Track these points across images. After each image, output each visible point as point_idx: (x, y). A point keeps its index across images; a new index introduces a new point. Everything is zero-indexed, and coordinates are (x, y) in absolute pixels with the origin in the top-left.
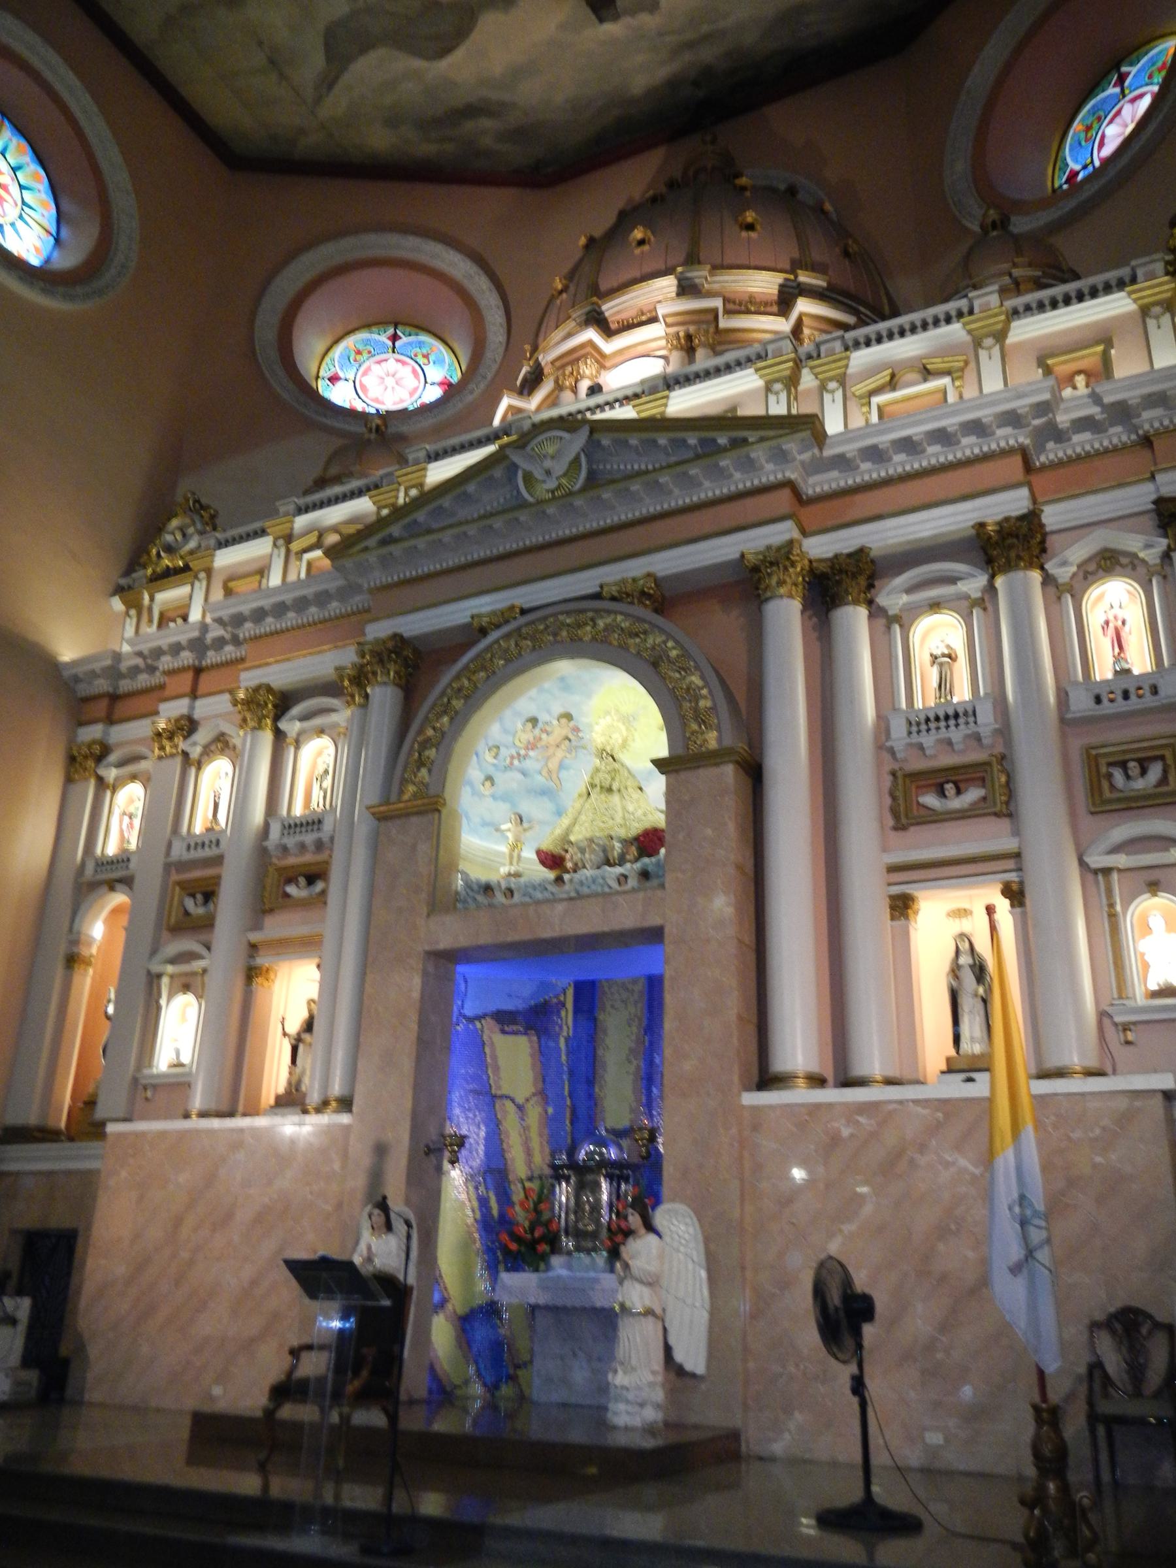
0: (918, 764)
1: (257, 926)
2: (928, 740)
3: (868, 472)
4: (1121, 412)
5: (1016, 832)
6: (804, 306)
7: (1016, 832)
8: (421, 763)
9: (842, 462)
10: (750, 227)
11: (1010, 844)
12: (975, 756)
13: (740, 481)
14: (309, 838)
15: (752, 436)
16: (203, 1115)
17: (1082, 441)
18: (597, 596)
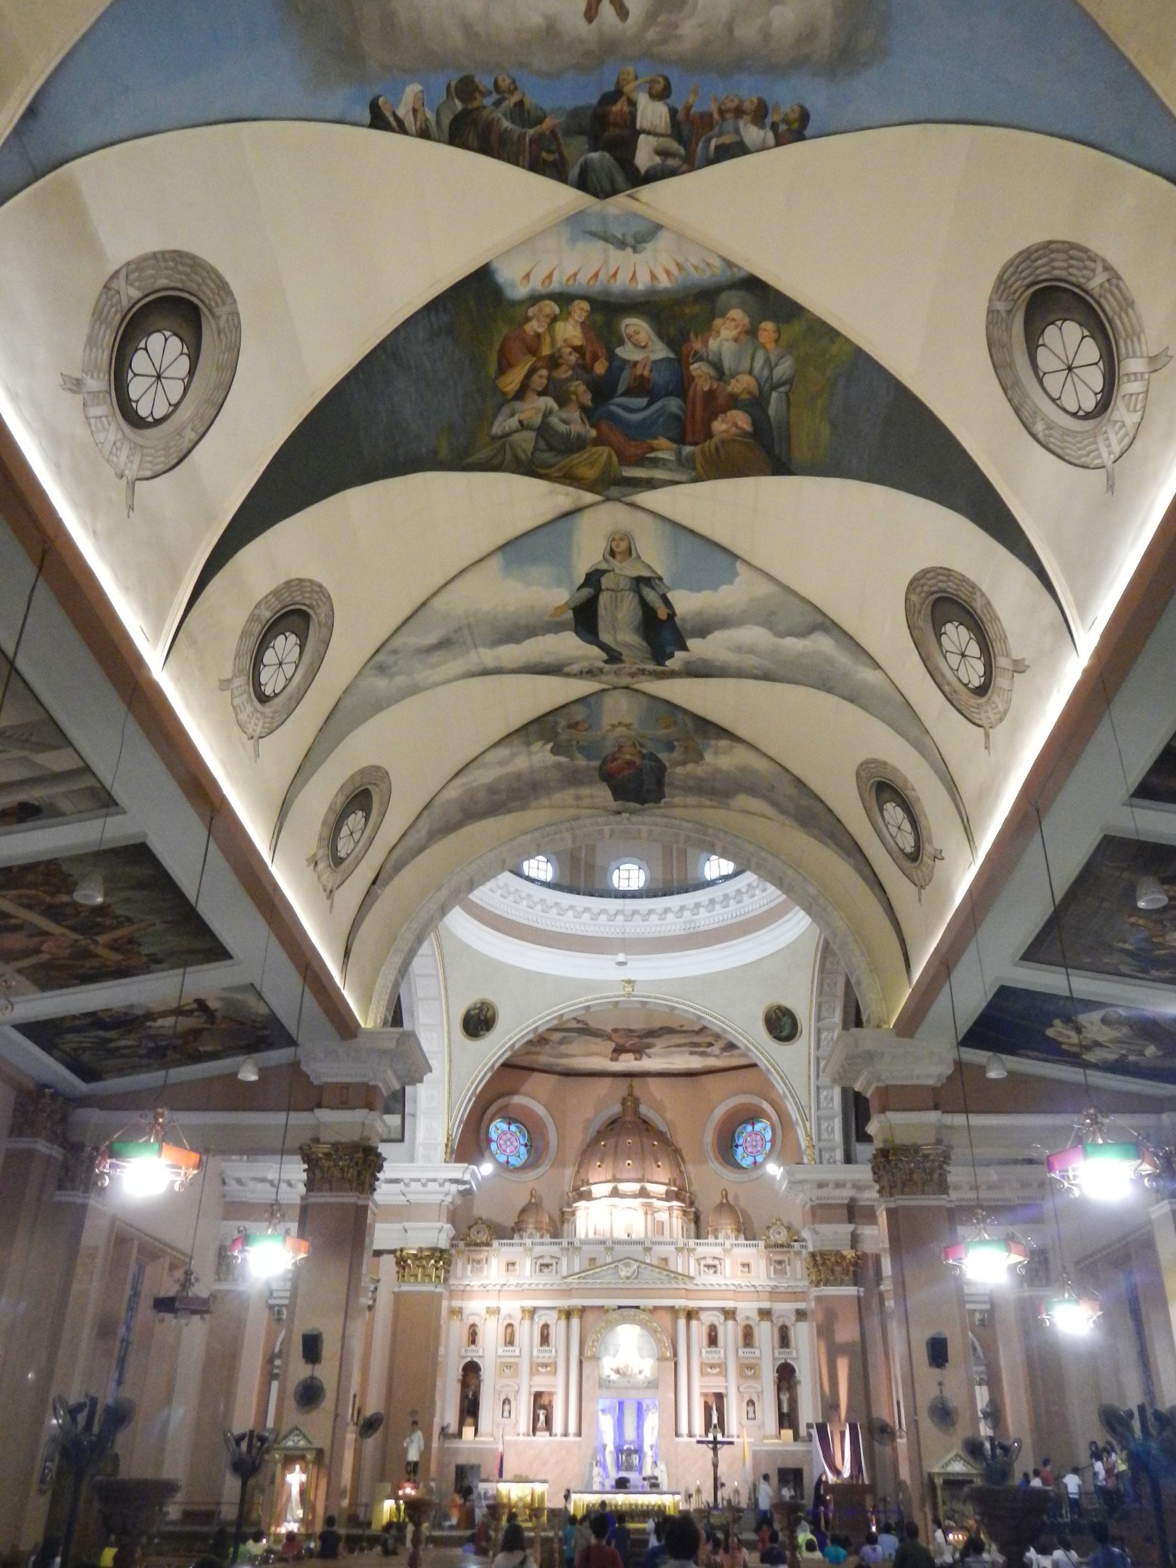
0: (707, 1361)
1: (531, 1379)
2: (710, 1356)
3: (702, 1288)
4: (753, 1286)
5: (726, 1381)
6: (676, 1204)
7: (726, 1381)
8: (593, 1346)
9: (697, 1285)
10: (659, 1166)
11: (725, 1384)
12: (718, 1361)
13: (675, 1286)
14: (547, 1355)
15: (680, 1277)
16: (524, 1435)
17: (746, 1289)
18: (638, 1307)
